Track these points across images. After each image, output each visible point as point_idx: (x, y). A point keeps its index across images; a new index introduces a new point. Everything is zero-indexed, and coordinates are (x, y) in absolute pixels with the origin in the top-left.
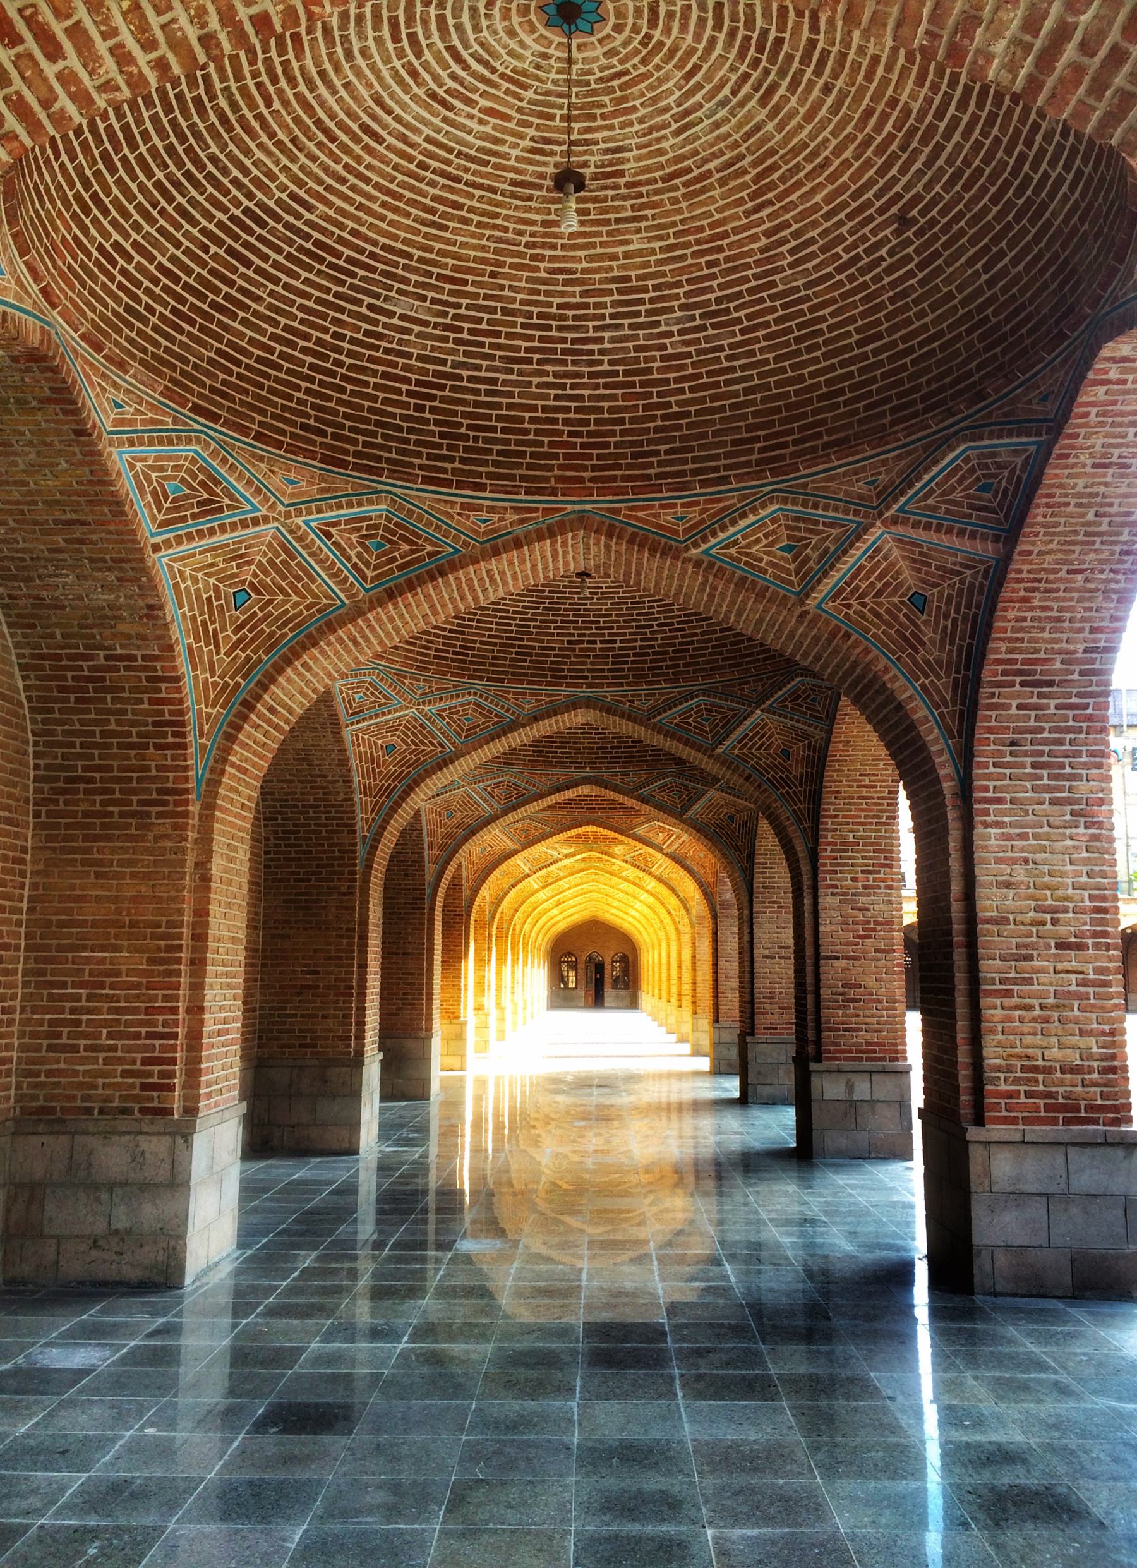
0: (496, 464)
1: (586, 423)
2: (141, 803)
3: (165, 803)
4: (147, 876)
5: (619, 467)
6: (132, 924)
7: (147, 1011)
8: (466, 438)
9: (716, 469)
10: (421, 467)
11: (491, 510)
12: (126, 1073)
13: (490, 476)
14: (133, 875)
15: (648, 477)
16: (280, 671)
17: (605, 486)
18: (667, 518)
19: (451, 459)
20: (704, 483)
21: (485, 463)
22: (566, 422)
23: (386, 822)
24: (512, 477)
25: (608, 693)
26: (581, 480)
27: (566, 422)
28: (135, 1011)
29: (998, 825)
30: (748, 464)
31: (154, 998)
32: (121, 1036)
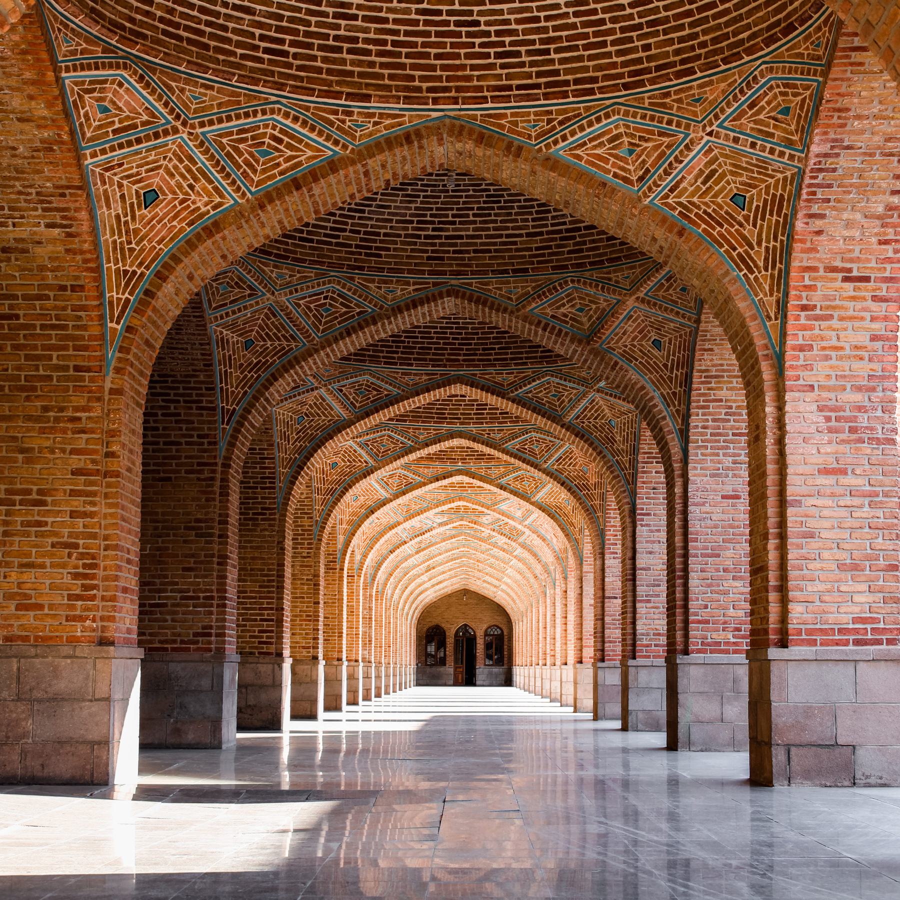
0: (418, 353)
1: (461, 334)
2: (254, 514)
3: (265, 514)
4: (258, 548)
5: (476, 355)
6: (252, 570)
7: (260, 609)
8: (404, 342)
9: (521, 358)
10: (384, 357)
11: (415, 375)
12: (251, 637)
13: (415, 359)
14: (251, 547)
15: (490, 360)
16: (316, 451)
17: (470, 363)
18: (499, 379)
19: (397, 353)
20: (516, 364)
21: (413, 353)
22: (451, 333)
24: (425, 360)
26: (458, 360)
27: (451, 333)
28: (254, 609)
29: (647, 525)
30: (535, 358)
31: (263, 603)
32: (248, 620)
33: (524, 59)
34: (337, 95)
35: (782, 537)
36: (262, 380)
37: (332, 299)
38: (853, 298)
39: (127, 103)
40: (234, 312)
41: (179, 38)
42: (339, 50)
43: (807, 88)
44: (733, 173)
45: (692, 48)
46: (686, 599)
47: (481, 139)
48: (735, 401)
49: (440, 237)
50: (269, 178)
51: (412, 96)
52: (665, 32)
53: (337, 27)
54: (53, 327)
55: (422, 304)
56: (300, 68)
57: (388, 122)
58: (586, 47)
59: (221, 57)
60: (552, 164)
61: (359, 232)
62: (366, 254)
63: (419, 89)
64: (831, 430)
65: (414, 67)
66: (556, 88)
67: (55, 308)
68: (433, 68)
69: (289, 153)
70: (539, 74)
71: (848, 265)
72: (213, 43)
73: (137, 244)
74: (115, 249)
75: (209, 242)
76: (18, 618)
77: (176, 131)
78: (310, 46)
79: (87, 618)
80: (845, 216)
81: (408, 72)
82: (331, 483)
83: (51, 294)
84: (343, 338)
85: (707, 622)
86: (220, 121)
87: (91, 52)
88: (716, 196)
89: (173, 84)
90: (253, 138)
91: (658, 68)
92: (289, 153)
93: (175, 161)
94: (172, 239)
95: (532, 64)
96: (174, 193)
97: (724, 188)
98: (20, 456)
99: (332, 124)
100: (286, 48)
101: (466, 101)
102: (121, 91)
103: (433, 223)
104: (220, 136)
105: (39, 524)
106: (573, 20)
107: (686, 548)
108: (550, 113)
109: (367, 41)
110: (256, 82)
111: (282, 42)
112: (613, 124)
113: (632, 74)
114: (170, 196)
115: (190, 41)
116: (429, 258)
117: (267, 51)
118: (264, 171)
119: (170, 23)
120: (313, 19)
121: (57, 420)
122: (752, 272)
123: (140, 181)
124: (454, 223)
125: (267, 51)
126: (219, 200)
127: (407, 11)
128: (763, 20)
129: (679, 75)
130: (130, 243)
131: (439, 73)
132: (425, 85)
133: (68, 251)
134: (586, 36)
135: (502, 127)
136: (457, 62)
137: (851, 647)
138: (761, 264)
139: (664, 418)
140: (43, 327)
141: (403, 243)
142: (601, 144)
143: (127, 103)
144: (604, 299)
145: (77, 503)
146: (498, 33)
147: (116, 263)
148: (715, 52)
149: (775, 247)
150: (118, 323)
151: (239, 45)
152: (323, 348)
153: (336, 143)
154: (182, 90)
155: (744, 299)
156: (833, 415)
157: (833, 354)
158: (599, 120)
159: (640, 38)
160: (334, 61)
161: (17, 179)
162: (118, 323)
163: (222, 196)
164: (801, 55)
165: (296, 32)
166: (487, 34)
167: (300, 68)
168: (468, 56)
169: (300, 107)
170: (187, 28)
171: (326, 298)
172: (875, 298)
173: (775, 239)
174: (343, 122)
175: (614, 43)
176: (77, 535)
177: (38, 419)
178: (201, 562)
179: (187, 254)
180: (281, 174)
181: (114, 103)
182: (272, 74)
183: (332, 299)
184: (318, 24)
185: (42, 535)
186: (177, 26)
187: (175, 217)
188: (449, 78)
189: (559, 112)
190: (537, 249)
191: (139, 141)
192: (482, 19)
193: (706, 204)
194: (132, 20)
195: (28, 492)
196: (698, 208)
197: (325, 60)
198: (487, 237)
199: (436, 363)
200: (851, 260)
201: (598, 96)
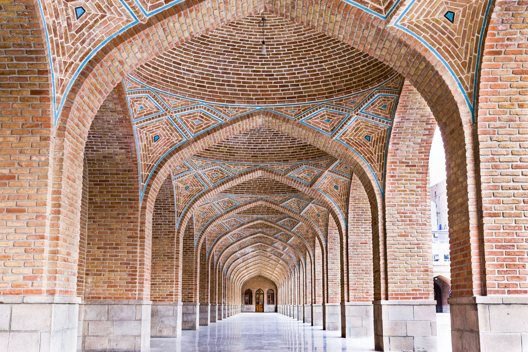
17: (265, 193)
18: (276, 199)
23: (213, 247)
25: (266, 217)
33: (290, 88)
34: (223, 101)
35: (386, 260)
36: (191, 201)
37: (217, 171)
38: (410, 173)
39: (149, 105)
40: (182, 177)
41: (167, 82)
42: (224, 85)
43: (393, 98)
44: (365, 128)
45: (351, 84)
46: (348, 281)
47: (275, 116)
48: (365, 208)
49: (256, 149)
50: (199, 131)
51: (249, 101)
52: (341, 78)
53: (223, 77)
54: (121, 185)
55: (250, 173)
56: (210, 92)
57: (241, 110)
58: (312, 83)
59: (182, 88)
60: (300, 125)
61: (227, 147)
62: (230, 155)
63: (252, 99)
64: (402, 221)
65: (250, 91)
66: (301, 98)
67: (122, 178)
68: (257, 91)
69: (206, 122)
70: (295, 93)
71: (408, 161)
72: (179, 83)
73: (152, 155)
74: (144, 156)
75: (177, 154)
76: (108, 290)
77: (166, 114)
78: (213, 84)
79: (133, 290)
80: (407, 143)
81: (248, 93)
82: (213, 237)
83: (121, 173)
84: (221, 185)
85: (356, 290)
86: (182, 111)
87: (137, 87)
88: (359, 136)
89: (165, 98)
90: (193, 117)
91: (338, 91)
92: (206, 122)
93: (166, 125)
94: (164, 153)
95: (293, 89)
96: (165, 136)
97: (362, 133)
98: (109, 231)
99: (221, 111)
100: (205, 84)
101: (269, 103)
102: (147, 101)
103: (254, 143)
104: (182, 116)
105: (116, 256)
106: (307, 74)
107: (348, 262)
108: (299, 107)
109: (233, 82)
110: (194, 97)
111: (203, 82)
112: (322, 111)
113: (329, 93)
114: (164, 138)
115: (171, 83)
116: (252, 156)
117: (198, 86)
118: (197, 128)
119: (164, 76)
120: (215, 74)
121: (122, 218)
122: (373, 164)
123: (153, 132)
124: (261, 143)
125: (198, 86)
126: (180, 139)
127: (248, 71)
128: (376, 74)
129: (346, 93)
130: (149, 154)
131: (259, 93)
132: (254, 97)
133: (127, 157)
134: (312, 79)
135: (282, 112)
136: (266, 89)
137: (411, 300)
138: (376, 161)
139: (339, 214)
140: (117, 185)
141: (243, 151)
142: (318, 118)
143: (149, 105)
144: (316, 171)
145: (130, 248)
146: (280, 79)
147: (144, 161)
148: (359, 85)
149: (381, 155)
150: (144, 183)
151: (188, 84)
152: (214, 189)
153: (223, 118)
154: (168, 100)
155: (370, 173)
156: (403, 215)
157: (403, 193)
158: (317, 109)
159: (331, 80)
160: (222, 89)
161: (109, 132)
162: (144, 183)
163: (182, 137)
164: (390, 87)
165: (208, 79)
166: (277, 79)
167: (210, 92)
168: (270, 87)
169: (210, 105)
170: (170, 78)
171: (215, 171)
172: (418, 173)
173: (381, 152)
174: (225, 111)
175: (322, 82)
176: (130, 260)
177: (115, 218)
178: (169, 268)
179: (169, 158)
180: (203, 129)
181: (144, 105)
182: (200, 94)
183: (217, 171)
184: (216, 76)
185: (117, 260)
186: (167, 77)
187: (165, 145)
188: (263, 95)
189: (302, 107)
190: (292, 153)
191: (153, 118)
192: (275, 74)
193: (356, 139)
194: (151, 76)
195: (112, 244)
196: (353, 140)
197: (219, 89)
198: (273, 148)
199: (253, 193)
200: (409, 159)
201: (317, 101)
